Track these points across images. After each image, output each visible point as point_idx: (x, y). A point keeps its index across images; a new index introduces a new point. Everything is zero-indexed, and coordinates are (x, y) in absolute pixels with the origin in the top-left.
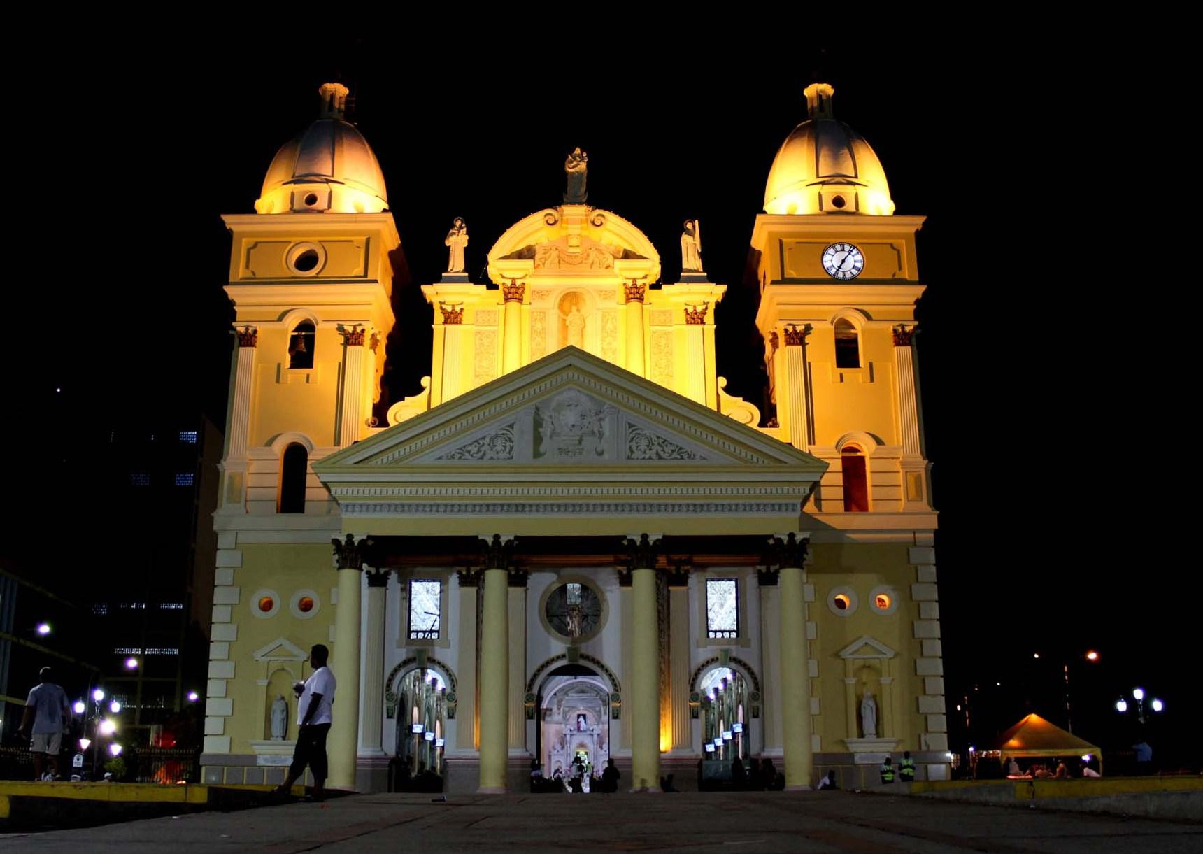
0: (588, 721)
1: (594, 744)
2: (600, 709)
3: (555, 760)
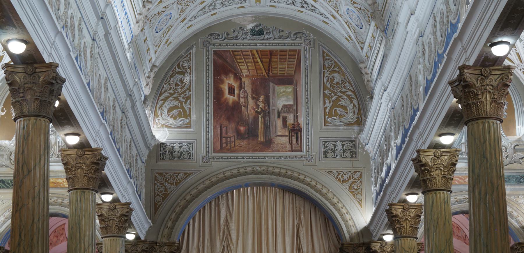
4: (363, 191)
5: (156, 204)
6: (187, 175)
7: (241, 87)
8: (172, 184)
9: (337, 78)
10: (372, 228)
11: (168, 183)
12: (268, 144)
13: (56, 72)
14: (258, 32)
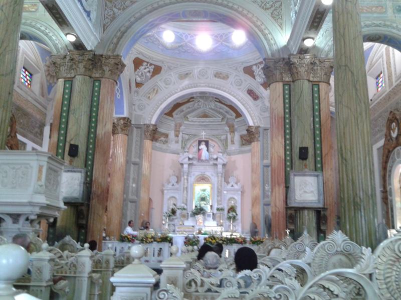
0: (211, 149)
1: (218, 176)
2: (227, 137)
3: (168, 197)
4: (283, 17)
5: (104, 25)
8: (119, 9)
10: (290, 47)
11: (117, 8)
13: (121, 60)
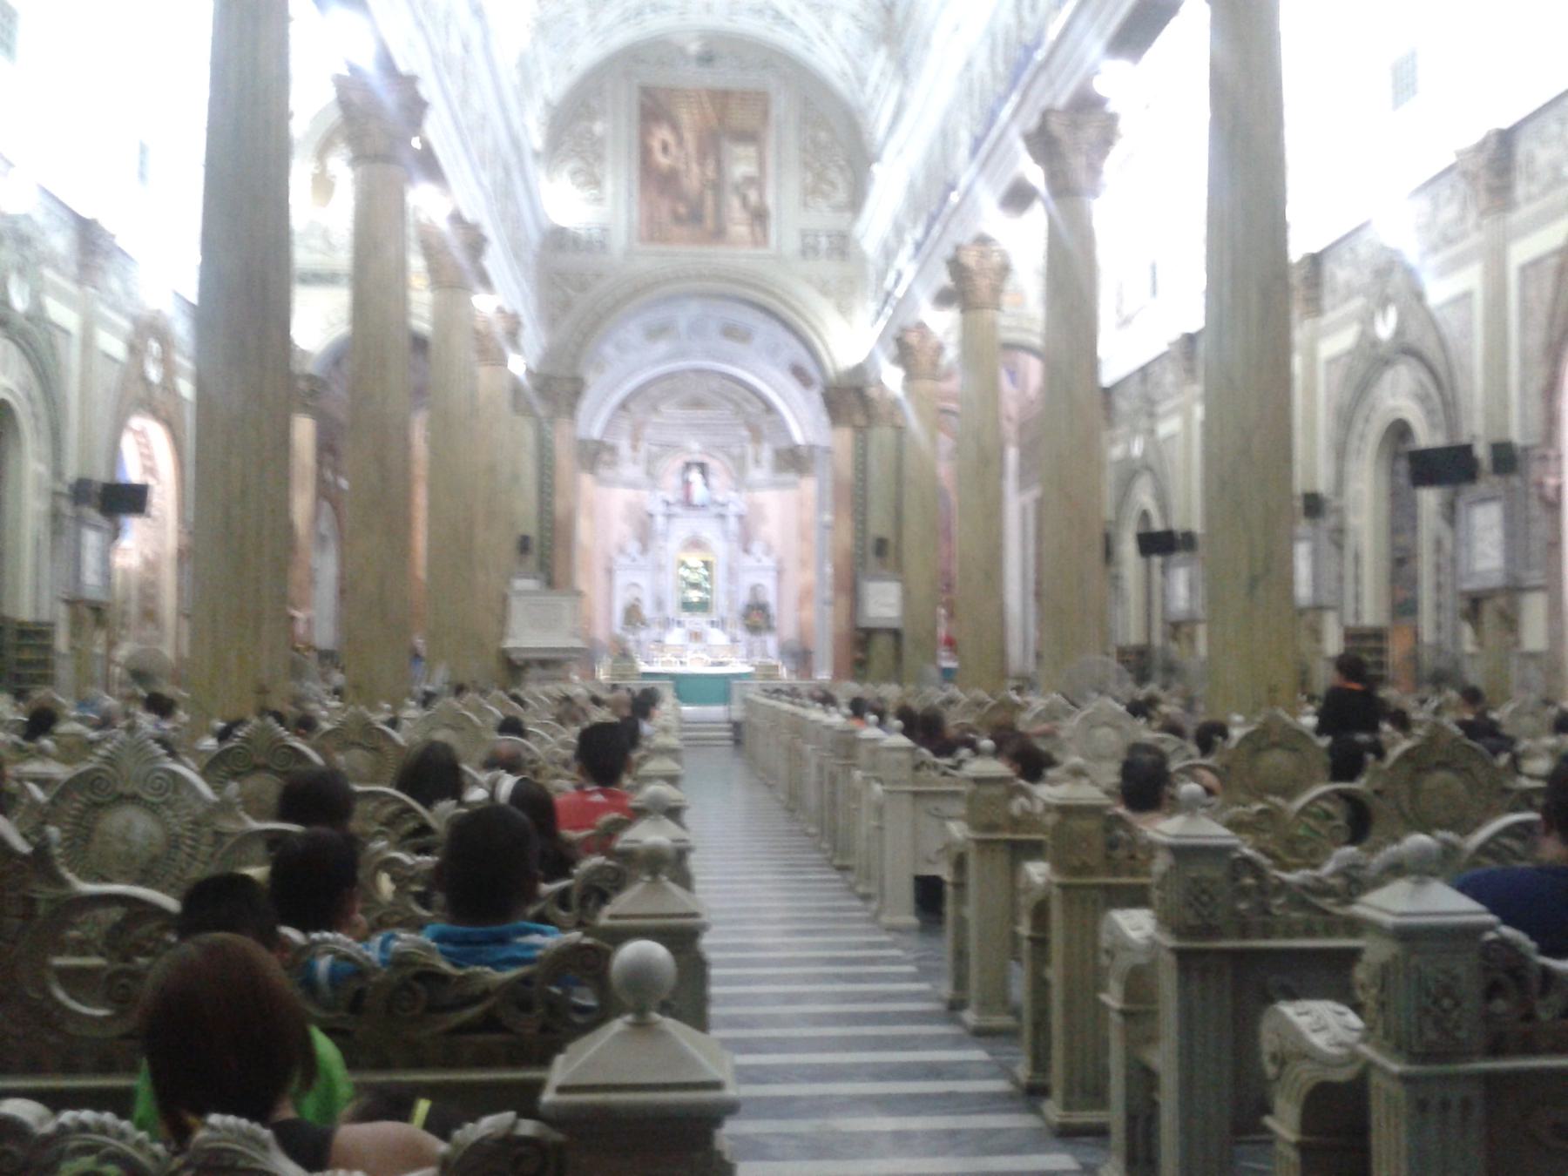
0: (713, 481)
6: (598, 276)
7: (680, 141)
9: (823, 136)
12: (719, 234)
14: (707, 59)
